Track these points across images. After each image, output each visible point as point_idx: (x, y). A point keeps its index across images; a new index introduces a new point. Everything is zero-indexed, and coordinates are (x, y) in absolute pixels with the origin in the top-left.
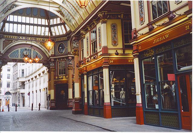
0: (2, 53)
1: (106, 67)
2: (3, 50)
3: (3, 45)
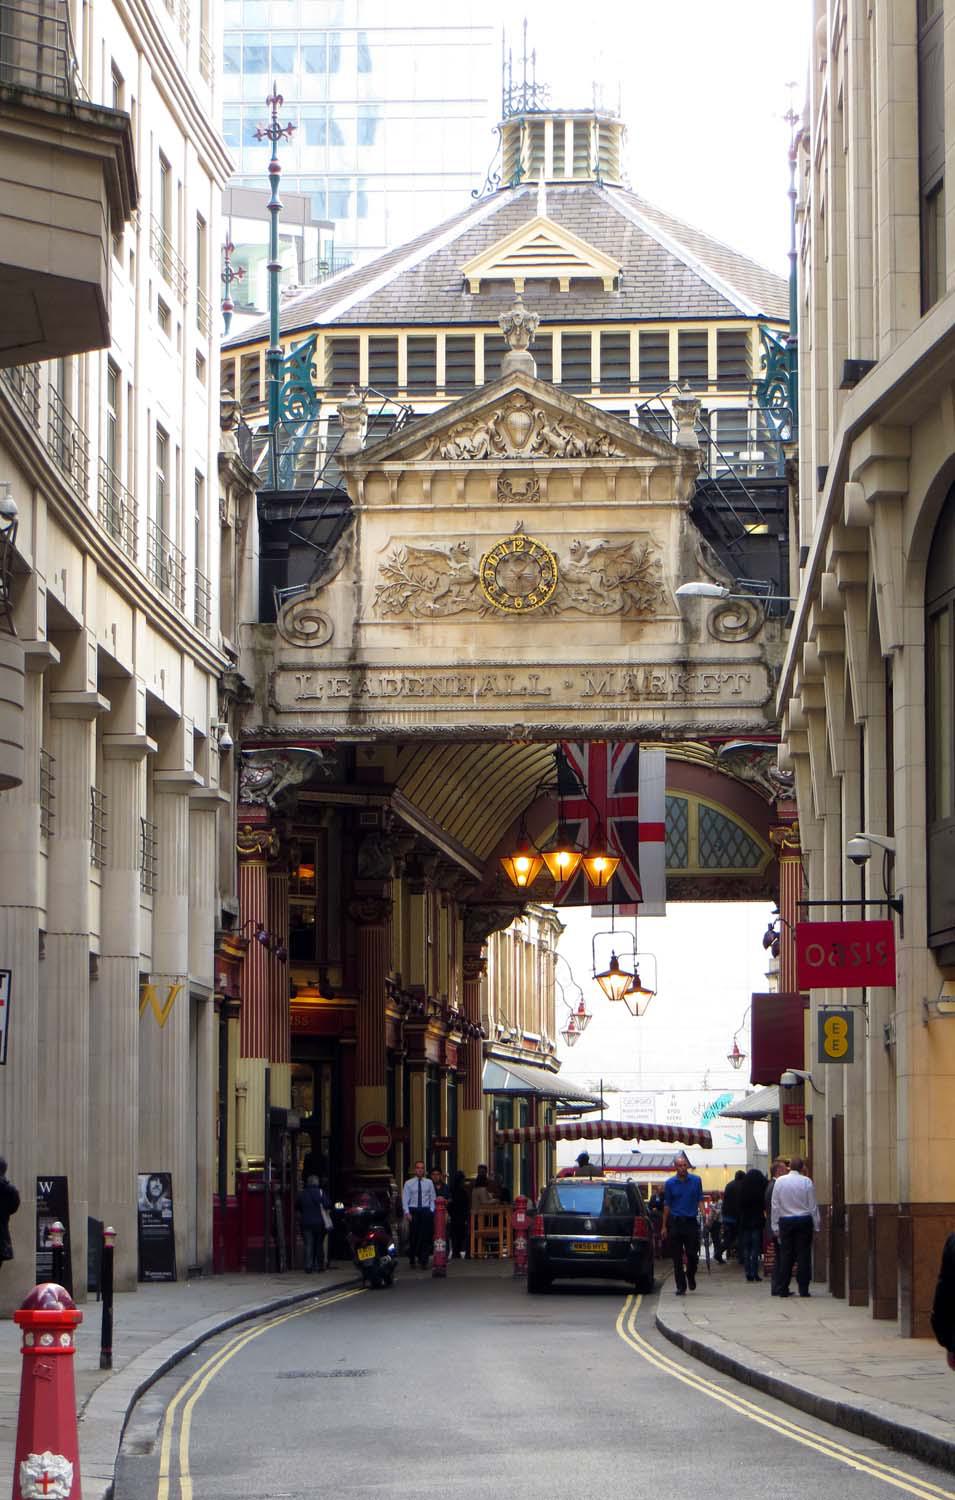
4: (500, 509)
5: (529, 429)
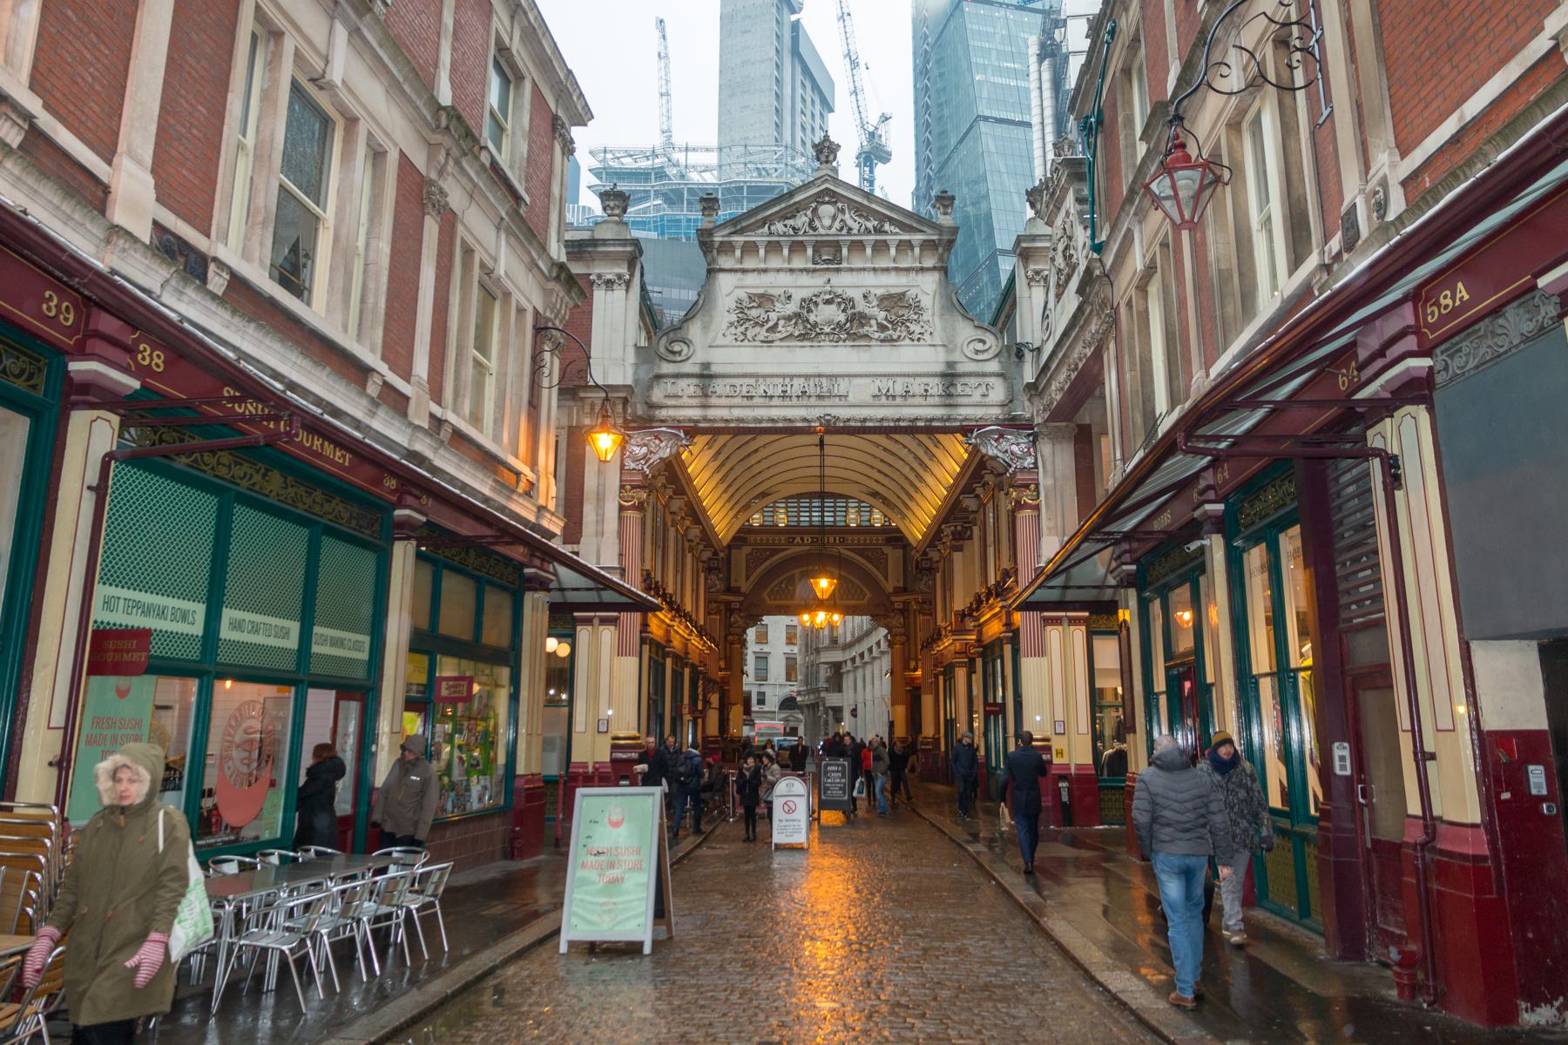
0: (743, 590)
1: (961, 665)
2: (747, 579)
3: (747, 567)
4: (815, 270)
5: (834, 218)
